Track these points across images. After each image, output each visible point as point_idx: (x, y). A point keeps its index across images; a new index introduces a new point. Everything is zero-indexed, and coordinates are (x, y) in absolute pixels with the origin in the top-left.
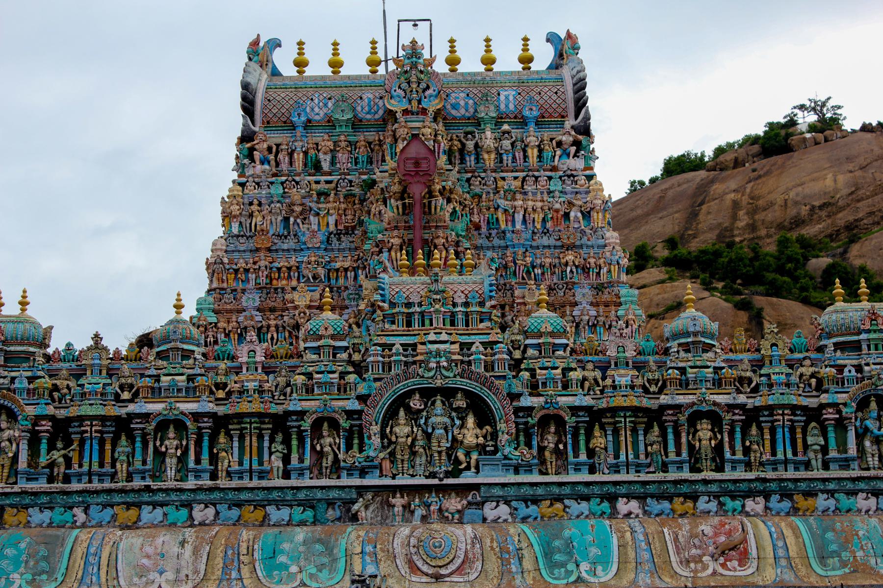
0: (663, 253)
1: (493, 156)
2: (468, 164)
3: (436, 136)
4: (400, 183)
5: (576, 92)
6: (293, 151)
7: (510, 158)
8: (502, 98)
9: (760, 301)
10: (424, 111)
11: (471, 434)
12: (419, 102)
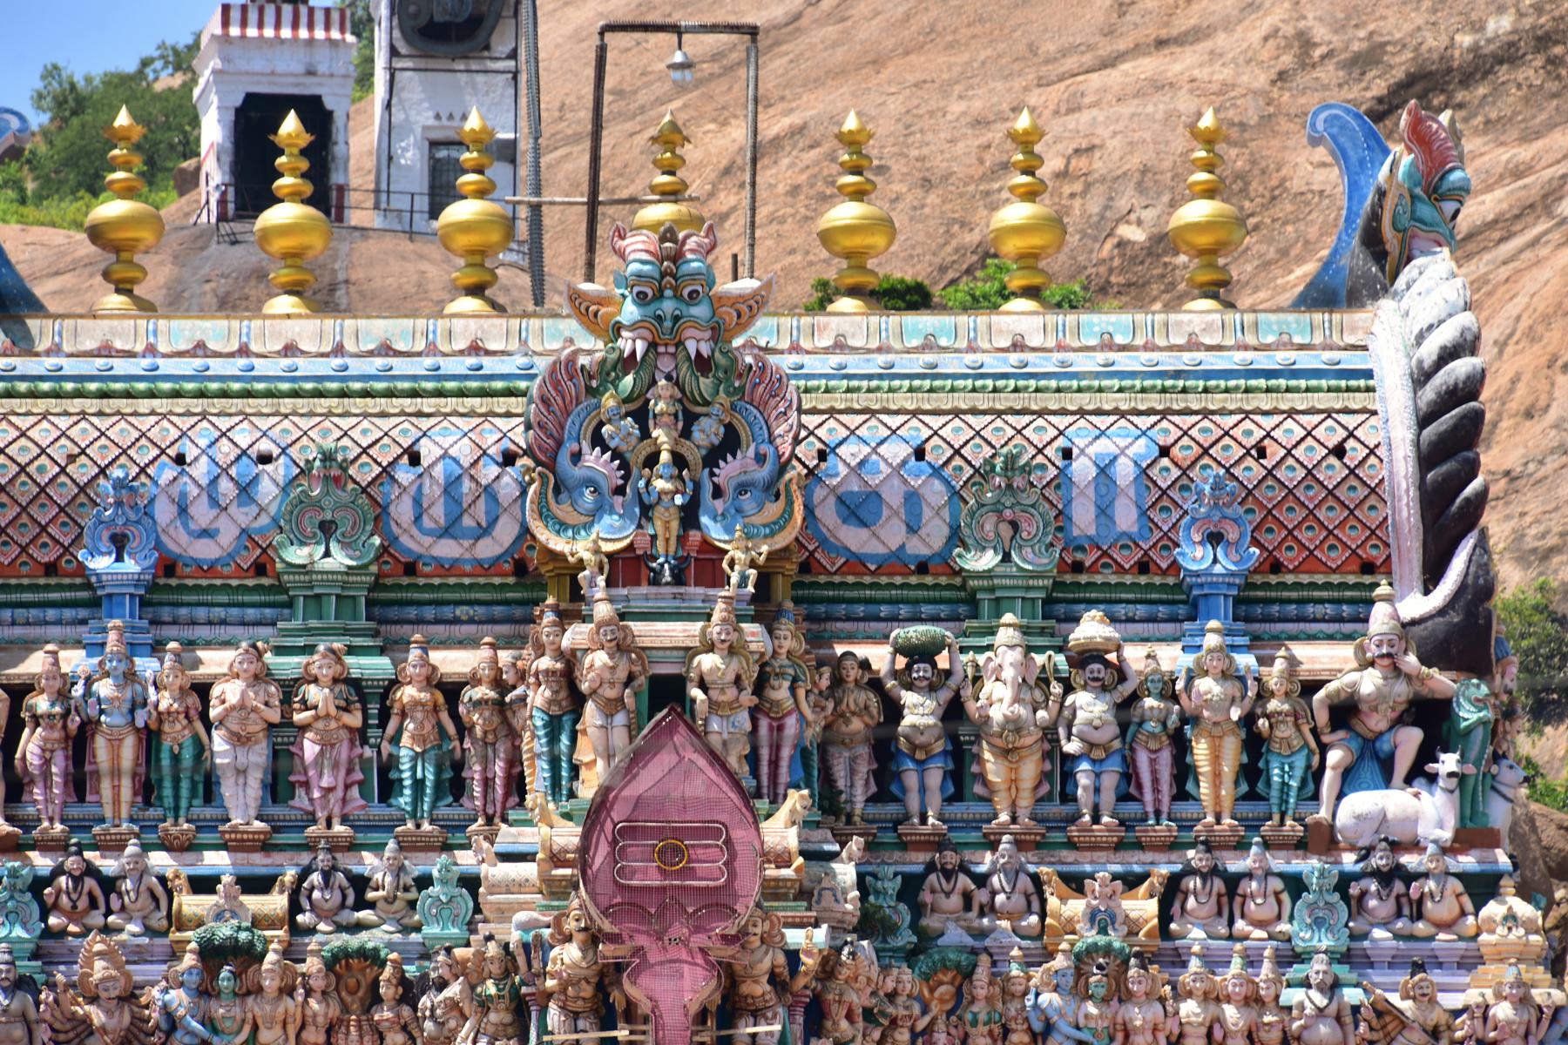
1: (1029, 770)
2: (913, 803)
3: (760, 686)
4: (593, 938)
5: (1427, 459)
6: (88, 729)
7: (1110, 781)
8: (1082, 469)
10: (704, 566)
12: (689, 516)
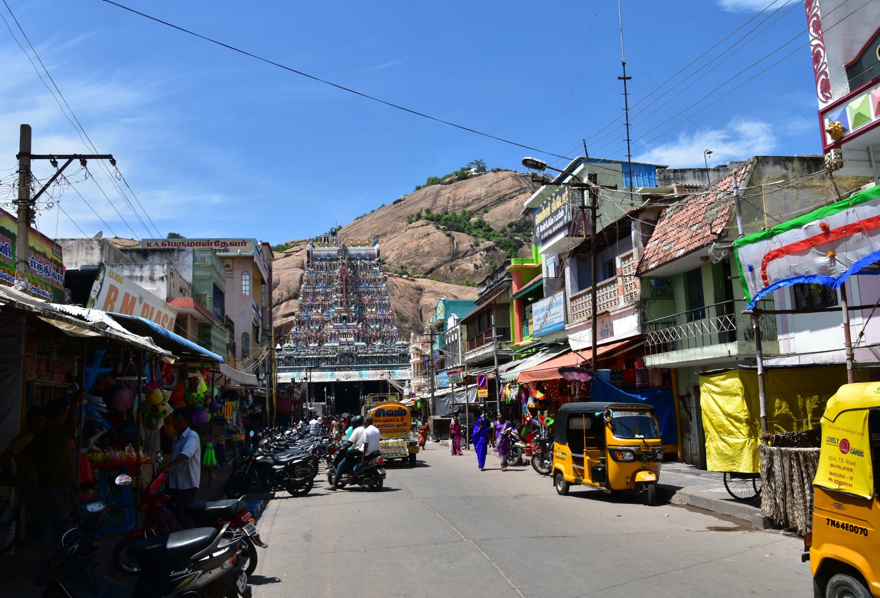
0: (424, 214)
9: (454, 233)
11: (351, 360)
